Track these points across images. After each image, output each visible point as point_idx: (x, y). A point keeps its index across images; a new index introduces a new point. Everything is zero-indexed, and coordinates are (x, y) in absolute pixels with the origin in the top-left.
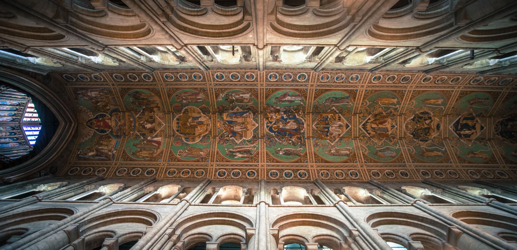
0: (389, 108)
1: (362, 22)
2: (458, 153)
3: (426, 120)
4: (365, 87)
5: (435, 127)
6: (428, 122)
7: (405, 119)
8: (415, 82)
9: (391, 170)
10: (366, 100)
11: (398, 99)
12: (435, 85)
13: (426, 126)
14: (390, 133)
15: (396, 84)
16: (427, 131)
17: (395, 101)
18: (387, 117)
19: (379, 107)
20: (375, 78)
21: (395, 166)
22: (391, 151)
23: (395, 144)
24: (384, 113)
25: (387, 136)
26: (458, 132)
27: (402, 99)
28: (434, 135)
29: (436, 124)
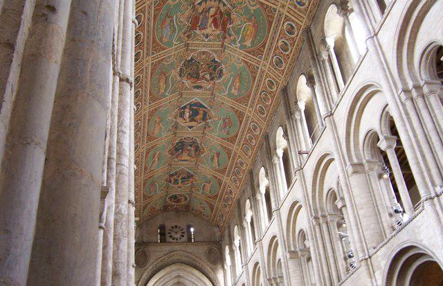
0: (237, 33)
1: (398, 101)
2: (161, 109)
3: (211, 74)
4: (281, 9)
5: (198, 84)
6: (208, 76)
7: (215, 52)
8: (271, 71)
9: (144, 39)
10: (258, 6)
11: (249, 47)
12: (260, 91)
13: (201, 75)
14: (198, 32)
15: (275, 50)
16: (195, 76)
17: (248, 43)
18: (224, 29)
19: (241, 21)
20: (292, 27)
21: (148, 44)
22: (171, 35)
23: (180, 39)
24: (229, 26)
25: (193, 27)
26: (188, 106)
27: (249, 53)
28: (187, 83)
29: (202, 85)
